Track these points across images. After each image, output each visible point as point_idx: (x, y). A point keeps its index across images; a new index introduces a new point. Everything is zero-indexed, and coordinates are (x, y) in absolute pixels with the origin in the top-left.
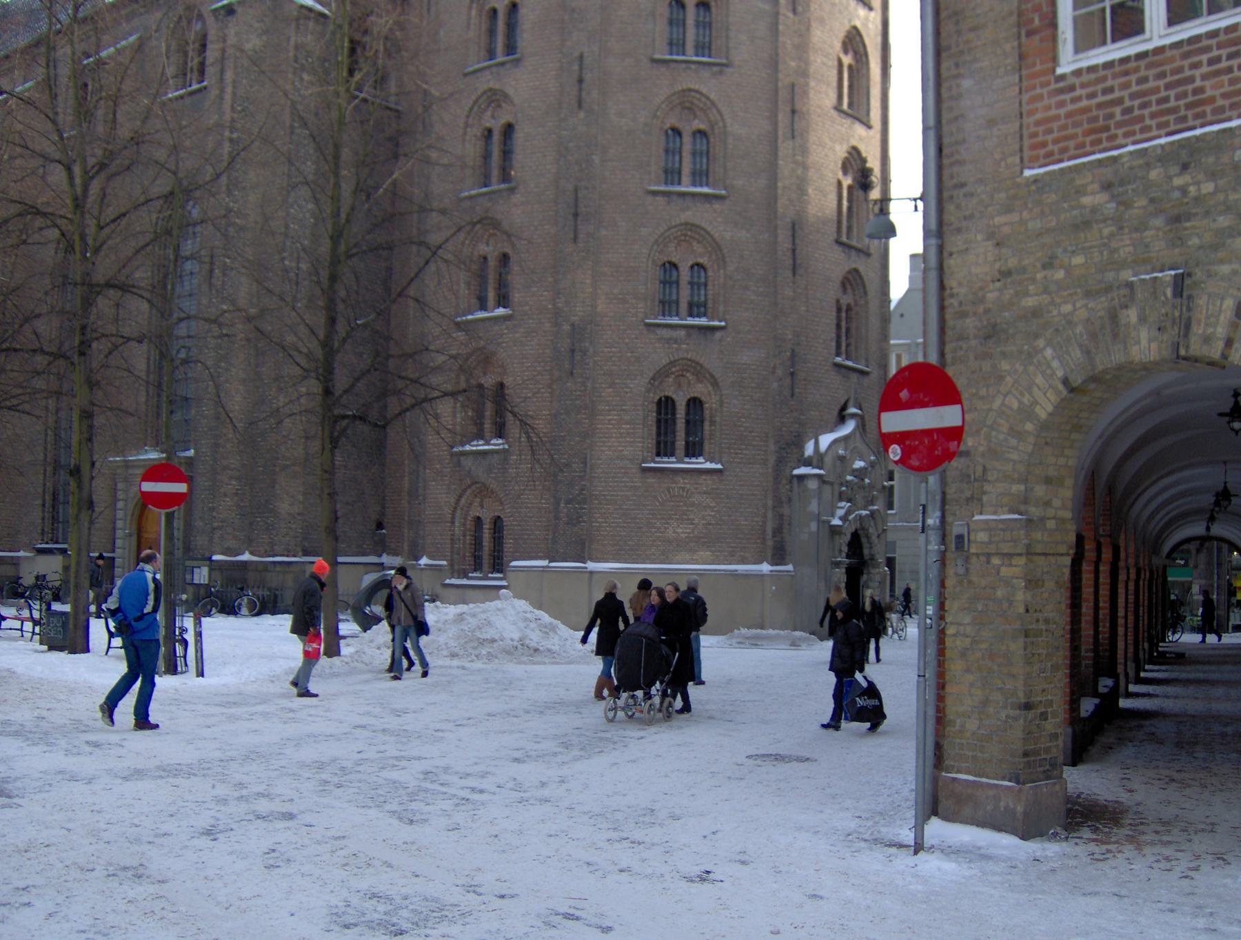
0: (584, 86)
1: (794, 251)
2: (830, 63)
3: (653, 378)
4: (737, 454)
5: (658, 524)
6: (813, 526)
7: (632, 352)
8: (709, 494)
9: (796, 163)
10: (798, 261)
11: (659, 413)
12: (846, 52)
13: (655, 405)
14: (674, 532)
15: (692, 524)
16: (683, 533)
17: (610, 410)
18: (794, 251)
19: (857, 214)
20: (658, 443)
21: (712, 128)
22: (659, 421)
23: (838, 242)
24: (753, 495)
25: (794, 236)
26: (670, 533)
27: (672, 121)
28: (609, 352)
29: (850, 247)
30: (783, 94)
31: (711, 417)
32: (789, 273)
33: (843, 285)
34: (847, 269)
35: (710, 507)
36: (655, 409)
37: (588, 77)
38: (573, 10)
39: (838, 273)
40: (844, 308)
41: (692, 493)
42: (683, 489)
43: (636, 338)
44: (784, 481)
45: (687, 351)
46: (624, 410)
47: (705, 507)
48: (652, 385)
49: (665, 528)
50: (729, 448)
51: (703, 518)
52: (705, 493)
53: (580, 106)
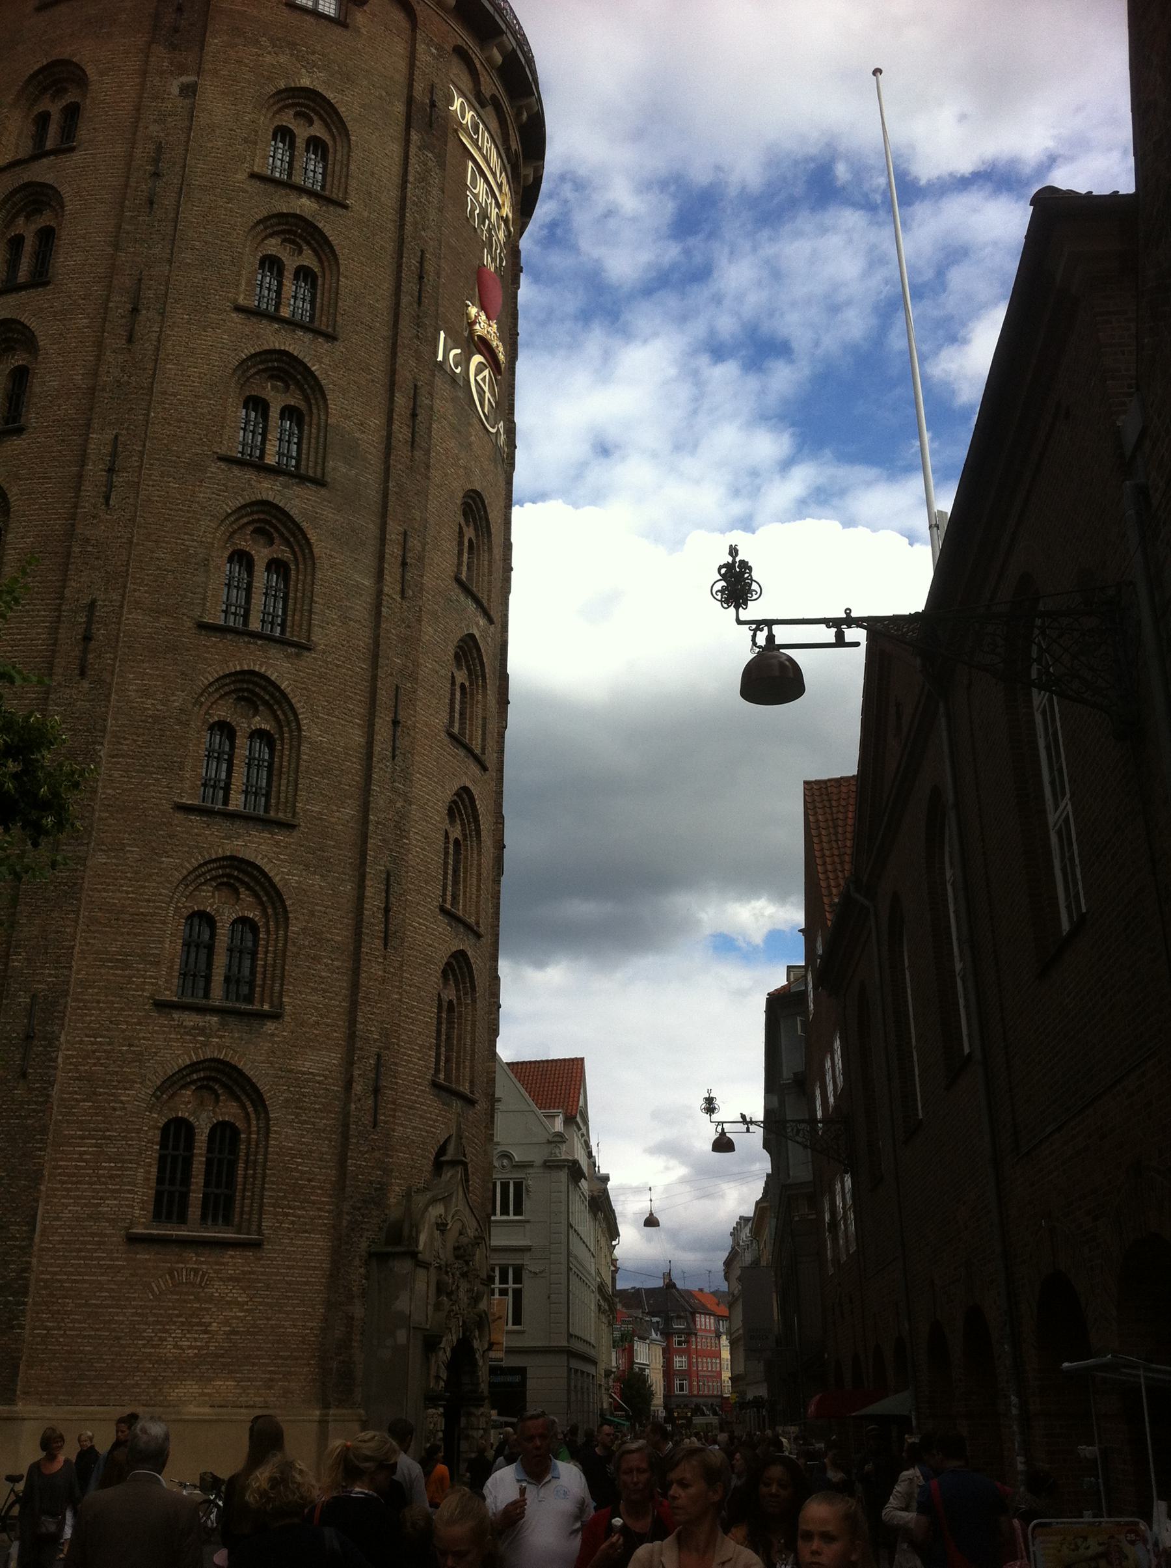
0: (93, 645)
1: (387, 910)
2: (443, 672)
3: (162, 1088)
4: (287, 1215)
5: (149, 1333)
6: (401, 1336)
7: (130, 1045)
8: (237, 1280)
9: (394, 790)
10: (392, 928)
11: (163, 1144)
12: (459, 667)
13: (158, 1132)
14: (176, 1346)
15: (206, 1332)
16: (190, 1347)
17: (82, 1138)
18: (387, 910)
19: (465, 881)
20: (159, 1195)
21: (282, 733)
22: (162, 1160)
23: (443, 910)
24: (306, 1283)
25: (387, 891)
26: (168, 1349)
27: (222, 712)
28: (92, 1044)
29: (459, 920)
30: (384, 697)
31: (247, 1155)
32: (378, 943)
33: (444, 972)
34: (454, 949)
35: (238, 1303)
36: (158, 1139)
37: (100, 633)
38: (87, 541)
39: (441, 956)
40: (445, 1005)
41: (211, 1279)
42: (196, 1271)
43: (140, 1024)
44: (357, 1262)
45: (220, 1048)
46: (109, 1138)
47: (228, 1303)
48: (158, 1098)
49: (162, 1339)
50: (274, 1206)
51: (226, 1322)
52: (231, 1279)
53: (83, 674)
